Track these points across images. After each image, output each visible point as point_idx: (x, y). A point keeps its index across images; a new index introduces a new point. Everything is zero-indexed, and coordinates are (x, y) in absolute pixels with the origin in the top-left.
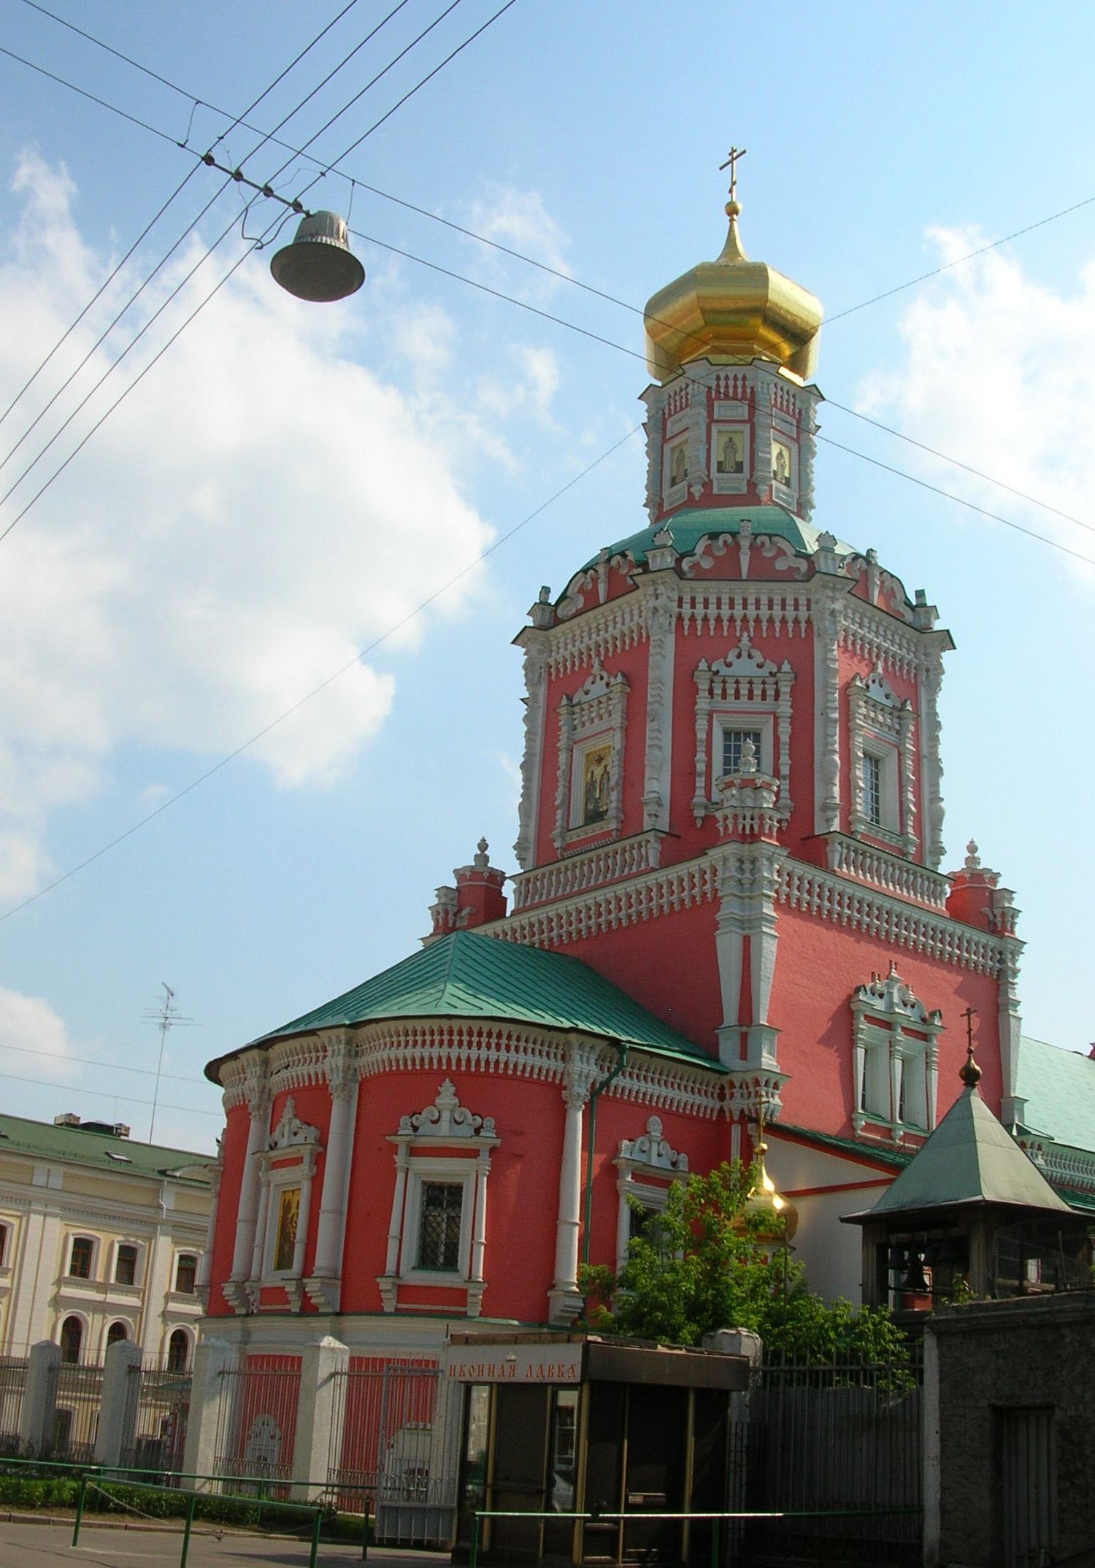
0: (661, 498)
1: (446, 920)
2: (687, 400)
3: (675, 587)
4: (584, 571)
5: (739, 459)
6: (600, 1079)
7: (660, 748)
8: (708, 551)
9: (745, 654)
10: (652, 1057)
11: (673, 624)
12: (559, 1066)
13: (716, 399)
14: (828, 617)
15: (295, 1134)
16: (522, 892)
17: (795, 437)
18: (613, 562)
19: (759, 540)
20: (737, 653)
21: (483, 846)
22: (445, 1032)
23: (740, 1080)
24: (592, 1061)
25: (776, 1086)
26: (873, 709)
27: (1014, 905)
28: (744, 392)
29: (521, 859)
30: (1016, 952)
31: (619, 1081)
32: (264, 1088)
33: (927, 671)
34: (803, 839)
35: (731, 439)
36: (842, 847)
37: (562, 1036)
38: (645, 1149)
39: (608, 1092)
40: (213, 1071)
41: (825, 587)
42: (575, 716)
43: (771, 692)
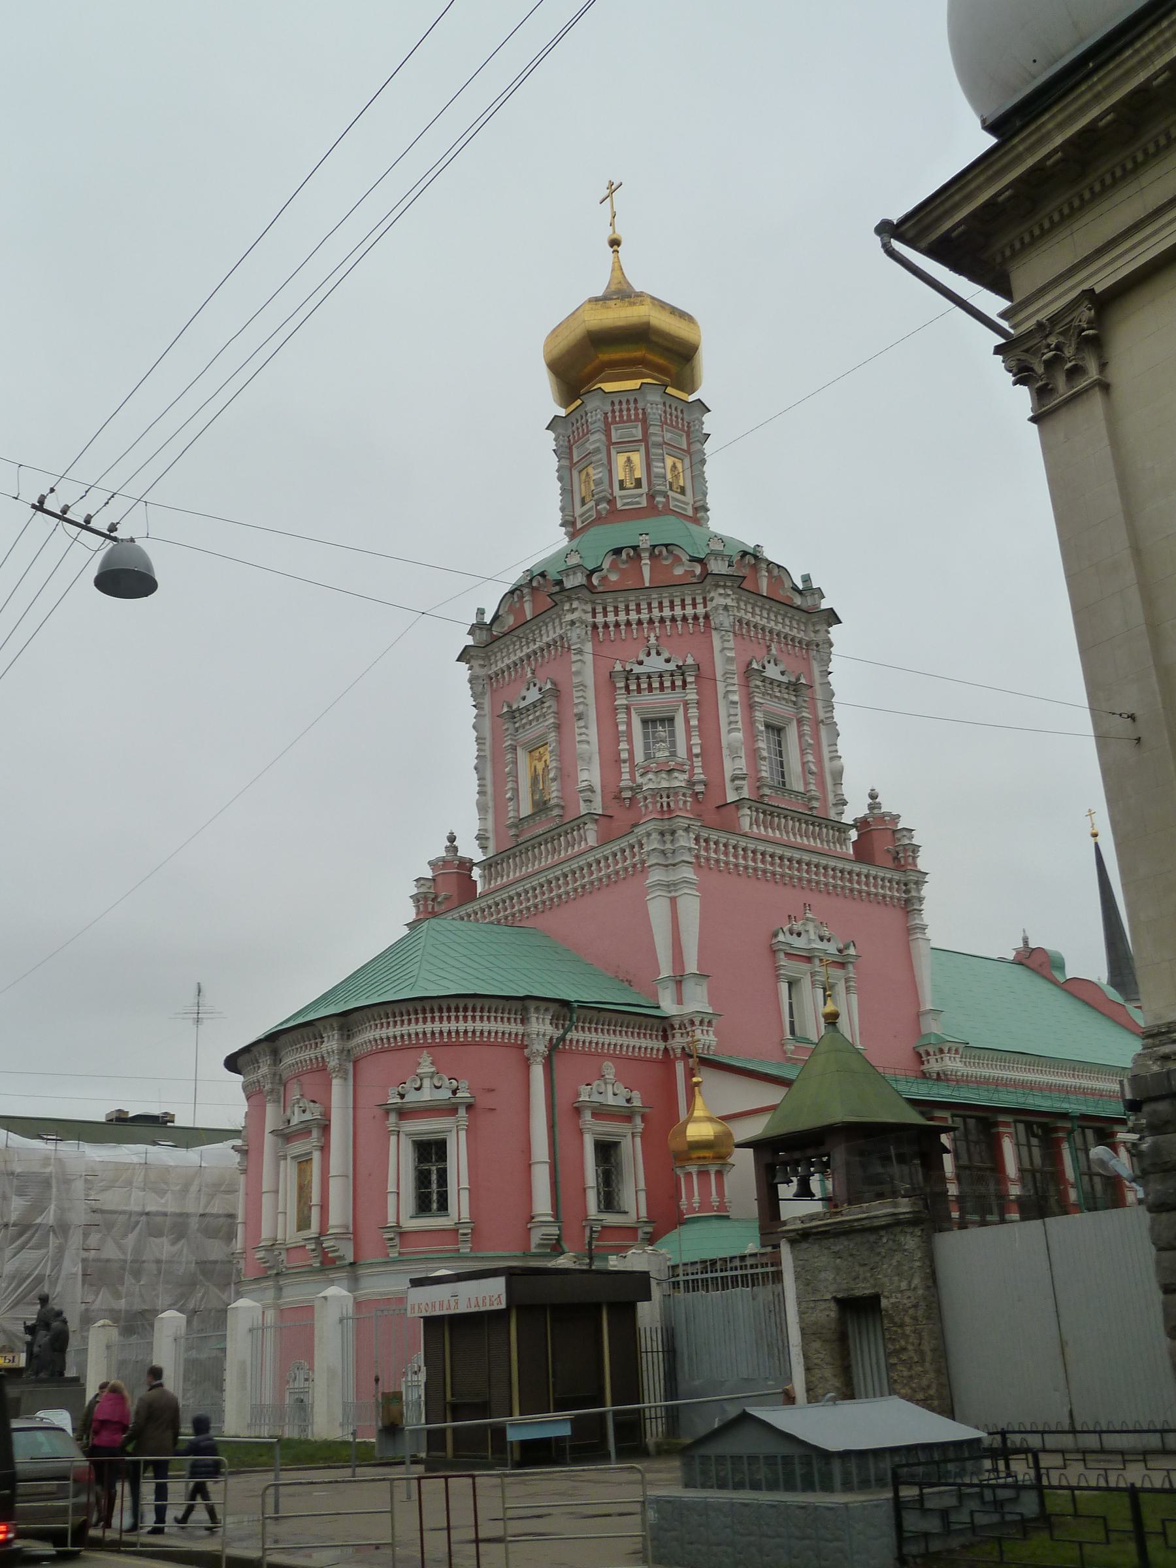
0: (573, 516)
1: (426, 906)
2: (588, 427)
4: (512, 592)
5: (638, 475)
6: (556, 1036)
7: (588, 742)
8: (613, 565)
9: (653, 652)
10: (599, 1012)
11: (589, 632)
12: (520, 1029)
13: (612, 424)
14: (721, 612)
15: (304, 1111)
16: (487, 878)
17: (685, 447)
18: (535, 584)
19: (656, 552)
20: (646, 652)
21: (452, 839)
22: (419, 1012)
23: (678, 1022)
24: (547, 1021)
25: (710, 1023)
26: (770, 686)
27: (914, 842)
28: (637, 415)
29: (484, 848)
30: (919, 883)
31: (573, 1035)
32: (275, 1074)
33: (817, 645)
34: (718, 807)
35: (629, 460)
36: (751, 811)
37: (518, 1004)
38: (601, 1091)
39: (564, 1045)
40: (233, 1063)
41: (717, 586)
42: (515, 720)
43: (679, 683)
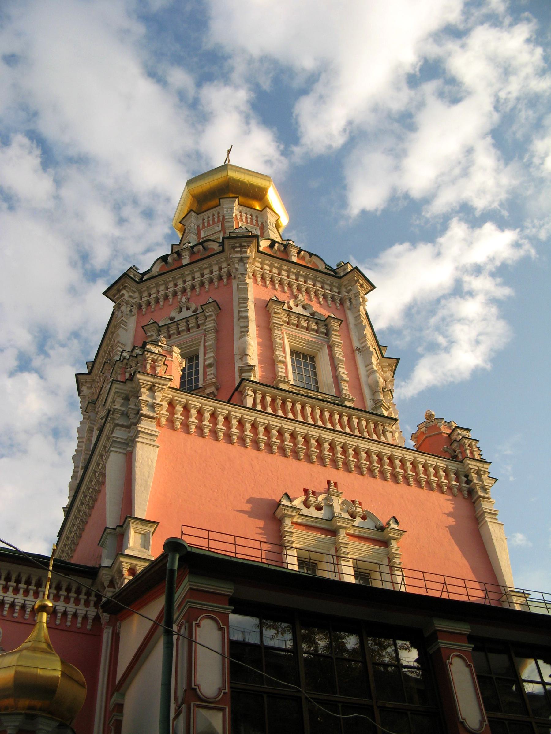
3: (136, 290)
9: (184, 309)
19: (195, 249)
20: (178, 310)
41: (234, 247)
